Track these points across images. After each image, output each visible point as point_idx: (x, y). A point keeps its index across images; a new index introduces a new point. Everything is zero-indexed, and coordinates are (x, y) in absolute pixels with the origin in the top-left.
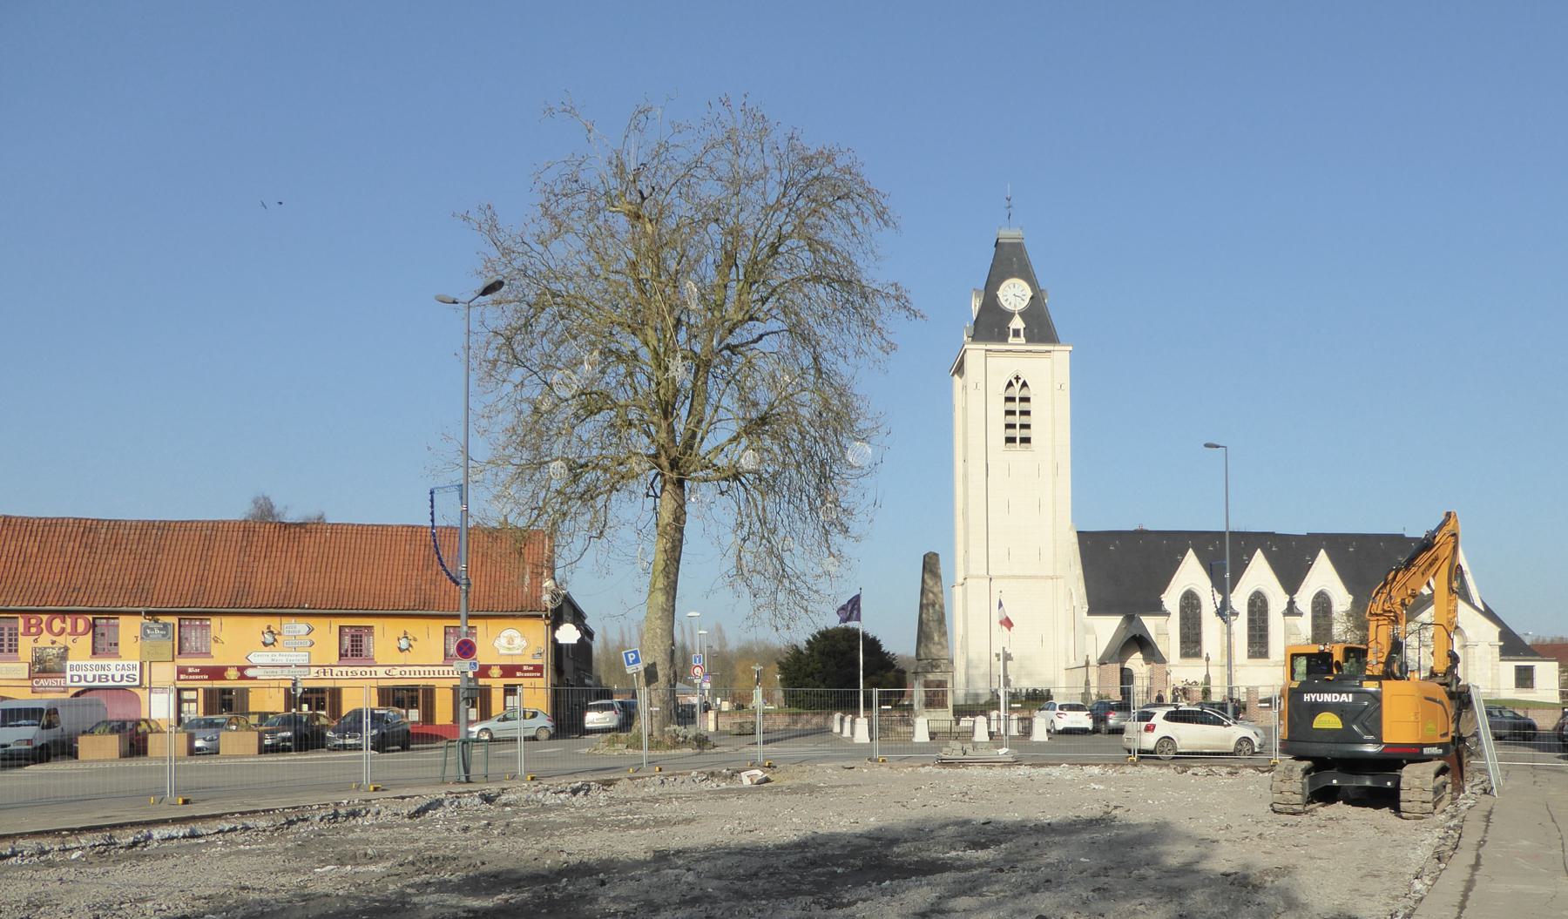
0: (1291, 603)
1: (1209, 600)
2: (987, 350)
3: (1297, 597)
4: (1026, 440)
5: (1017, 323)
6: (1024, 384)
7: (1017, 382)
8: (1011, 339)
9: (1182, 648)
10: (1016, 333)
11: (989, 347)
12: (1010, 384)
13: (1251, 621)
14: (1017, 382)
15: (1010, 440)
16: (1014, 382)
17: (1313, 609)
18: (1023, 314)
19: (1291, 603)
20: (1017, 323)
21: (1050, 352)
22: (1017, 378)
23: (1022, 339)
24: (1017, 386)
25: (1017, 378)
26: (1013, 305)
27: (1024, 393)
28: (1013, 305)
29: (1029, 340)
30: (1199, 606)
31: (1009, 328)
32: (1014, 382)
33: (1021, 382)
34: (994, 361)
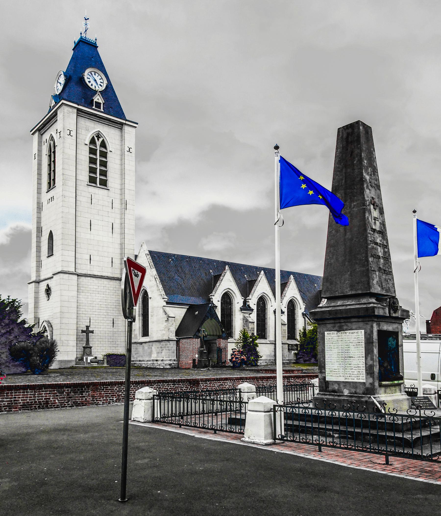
5: (98, 99)
7: (98, 140)
8: (94, 107)
10: (98, 105)
14: (98, 140)
16: (96, 138)
20: (98, 99)
23: (102, 110)
24: (98, 143)
25: (98, 137)
32: (96, 138)
33: (101, 140)
34: (85, 123)
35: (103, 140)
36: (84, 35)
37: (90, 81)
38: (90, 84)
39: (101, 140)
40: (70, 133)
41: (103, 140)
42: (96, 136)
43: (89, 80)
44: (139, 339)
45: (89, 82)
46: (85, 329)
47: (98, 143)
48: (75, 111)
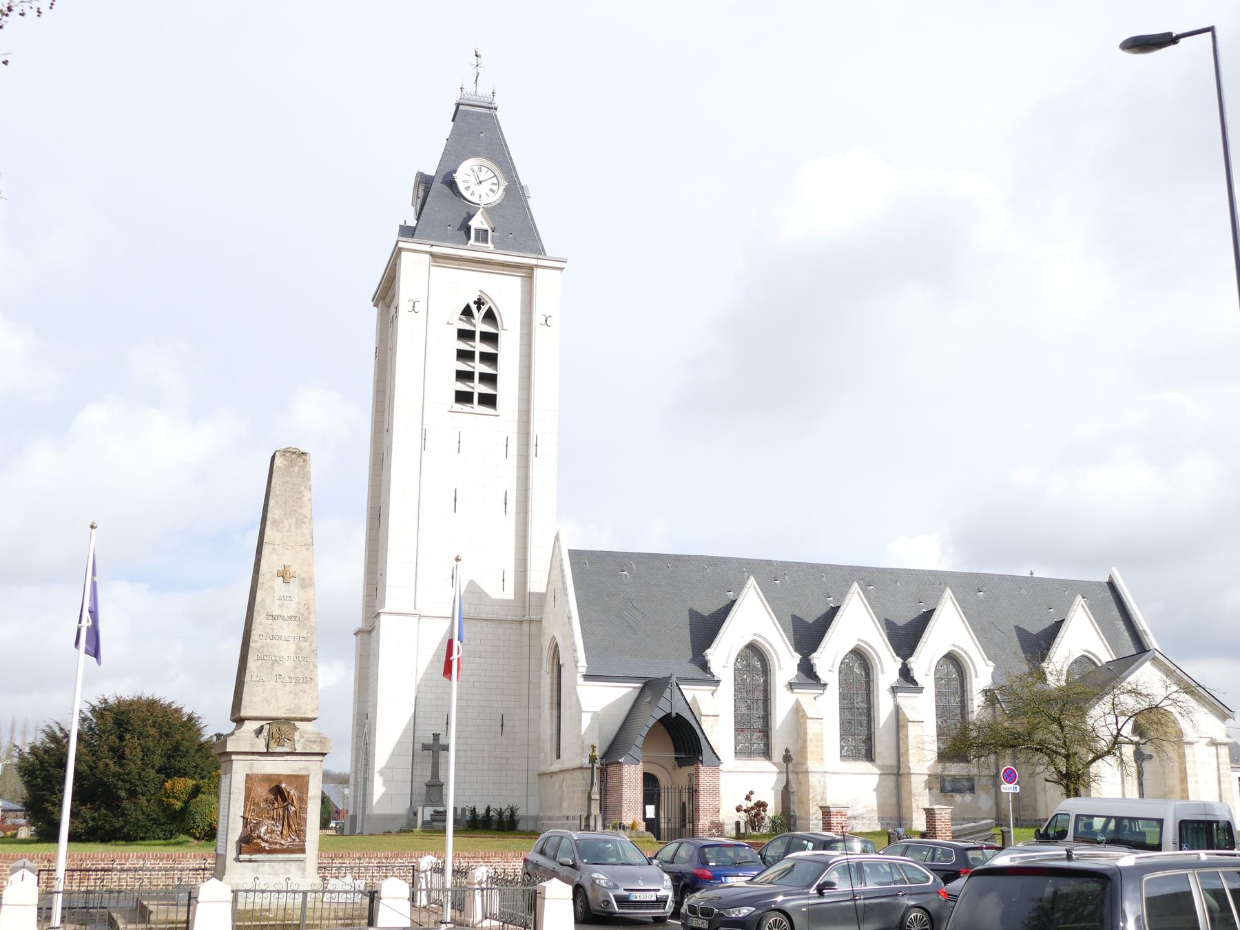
0: (905, 673)
1: (785, 663)
2: (433, 255)
3: (913, 662)
4: (489, 401)
6: (490, 316)
7: (479, 309)
9: (737, 743)
10: (482, 235)
11: (435, 250)
12: (467, 312)
13: (846, 698)
14: (479, 309)
15: (463, 398)
16: (474, 308)
17: (937, 680)
18: (491, 211)
19: (905, 673)
21: (531, 268)
22: (479, 303)
23: (490, 245)
24: (478, 315)
26: (476, 196)
27: (488, 329)
28: (476, 196)
29: (501, 245)
30: (766, 670)
31: (469, 228)
32: (474, 308)
33: (484, 309)
35: (490, 308)
36: (470, 88)
37: (469, 187)
38: (470, 192)
39: (484, 309)
40: (414, 307)
41: (490, 309)
42: (475, 303)
43: (466, 185)
44: (551, 765)
45: (466, 188)
46: (430, 741)
47: (478, 315)
48: (427, 257)
